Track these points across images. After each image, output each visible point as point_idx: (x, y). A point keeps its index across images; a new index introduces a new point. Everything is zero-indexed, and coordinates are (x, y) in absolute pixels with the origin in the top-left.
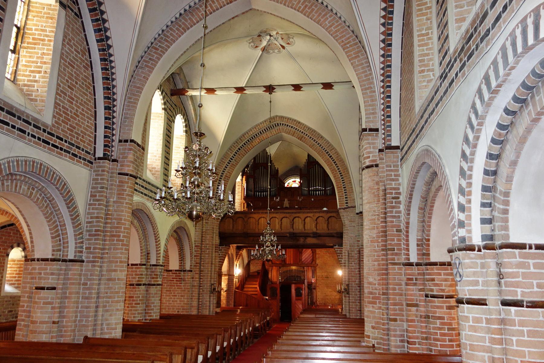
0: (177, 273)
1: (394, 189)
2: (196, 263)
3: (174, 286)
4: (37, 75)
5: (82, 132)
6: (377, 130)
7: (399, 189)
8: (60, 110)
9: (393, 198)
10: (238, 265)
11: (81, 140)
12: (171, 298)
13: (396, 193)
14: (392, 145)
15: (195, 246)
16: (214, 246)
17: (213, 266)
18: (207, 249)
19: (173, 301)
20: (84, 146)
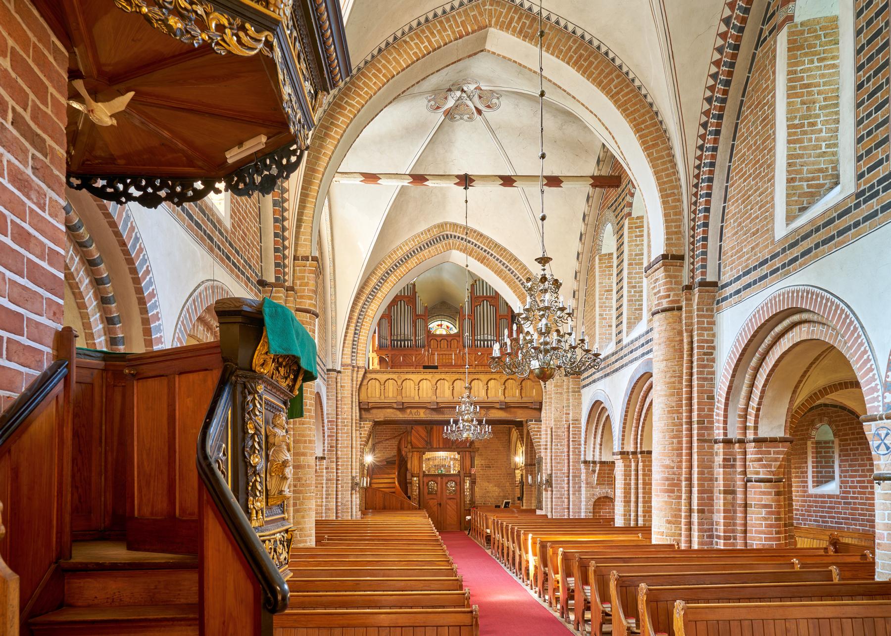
1: (707, 341)
2: (331, 447)
6: (682, 258)
7: (712, 342)
9: (705, 354)
13: (709, 347)
14: (708, 280)
15: (329, 422)
17: (354, 450)
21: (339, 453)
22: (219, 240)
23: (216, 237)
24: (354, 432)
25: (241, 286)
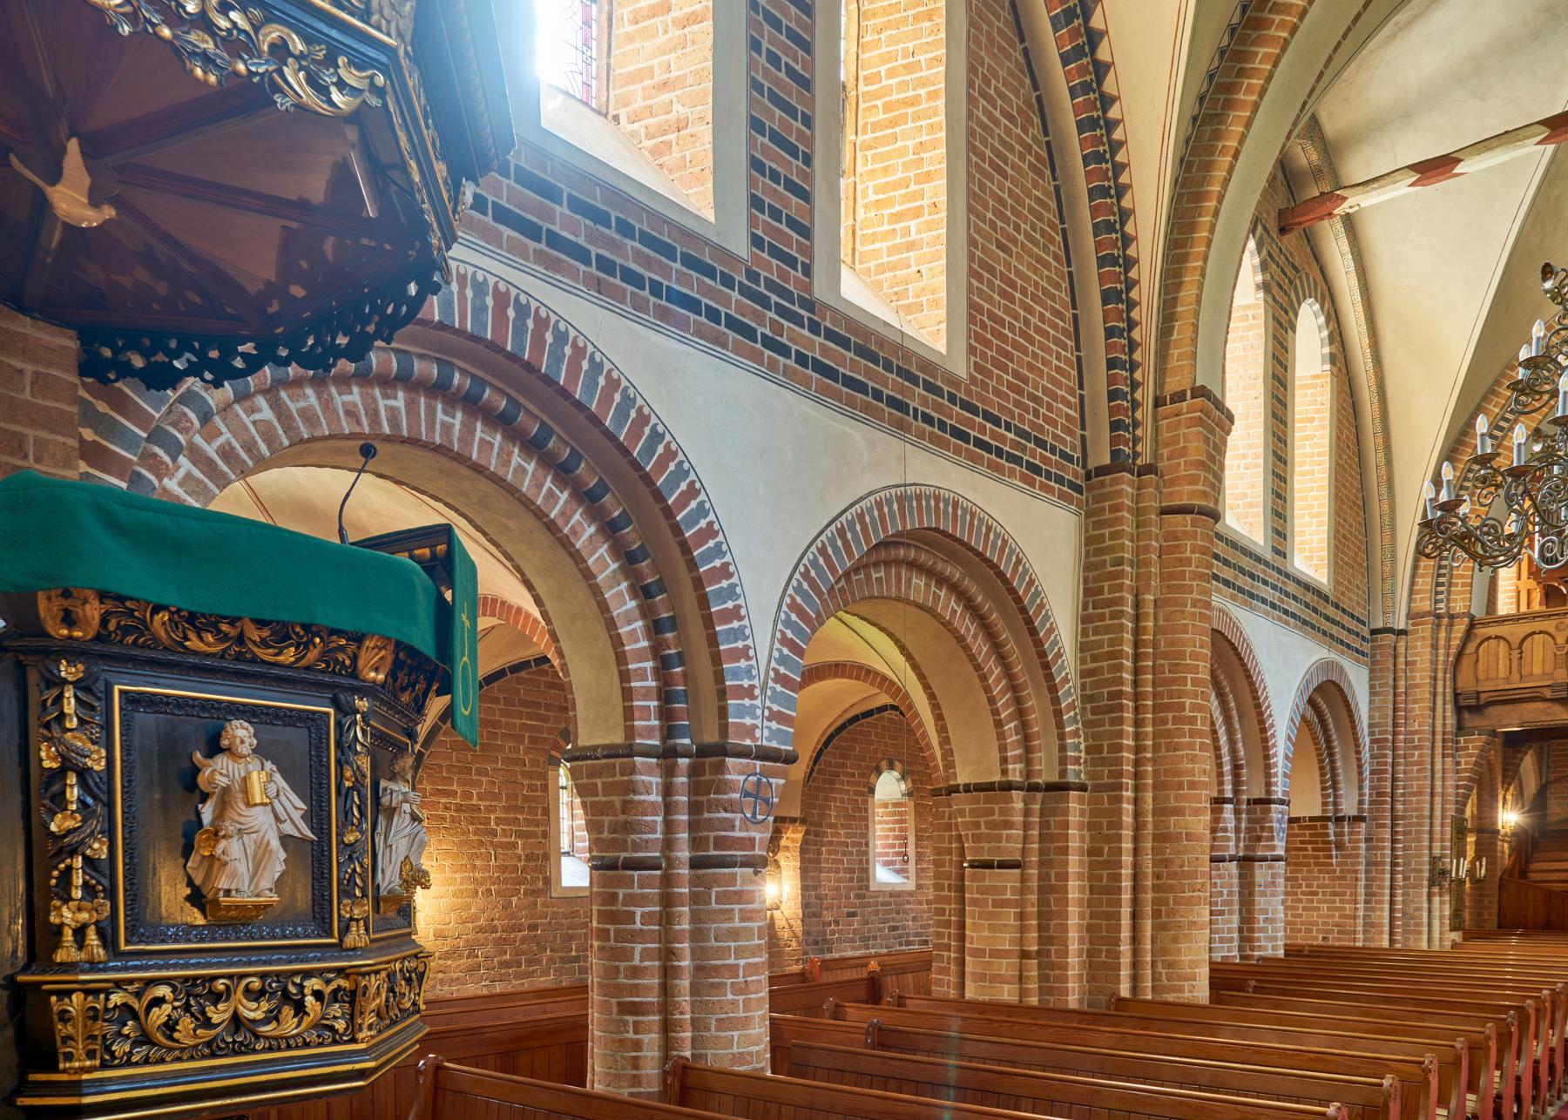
0: (1315, 827)
2: (1379, 794)
3: (1308, 865)
4: (913, 224)
5: (1046, 391)
8: (983, 325)
10: (1509, 797)
11: (1047, 419)
12: (1301, 901)
16: (1439, 737)
17: (1438, 799)
18: (1415, 748)
19: (1304, 909)
20: (1055, 437)
21: (1400, 807)
22: (925, 402)
23: (917, 398)
24: (1438, 759)
25: (1012, 486)
